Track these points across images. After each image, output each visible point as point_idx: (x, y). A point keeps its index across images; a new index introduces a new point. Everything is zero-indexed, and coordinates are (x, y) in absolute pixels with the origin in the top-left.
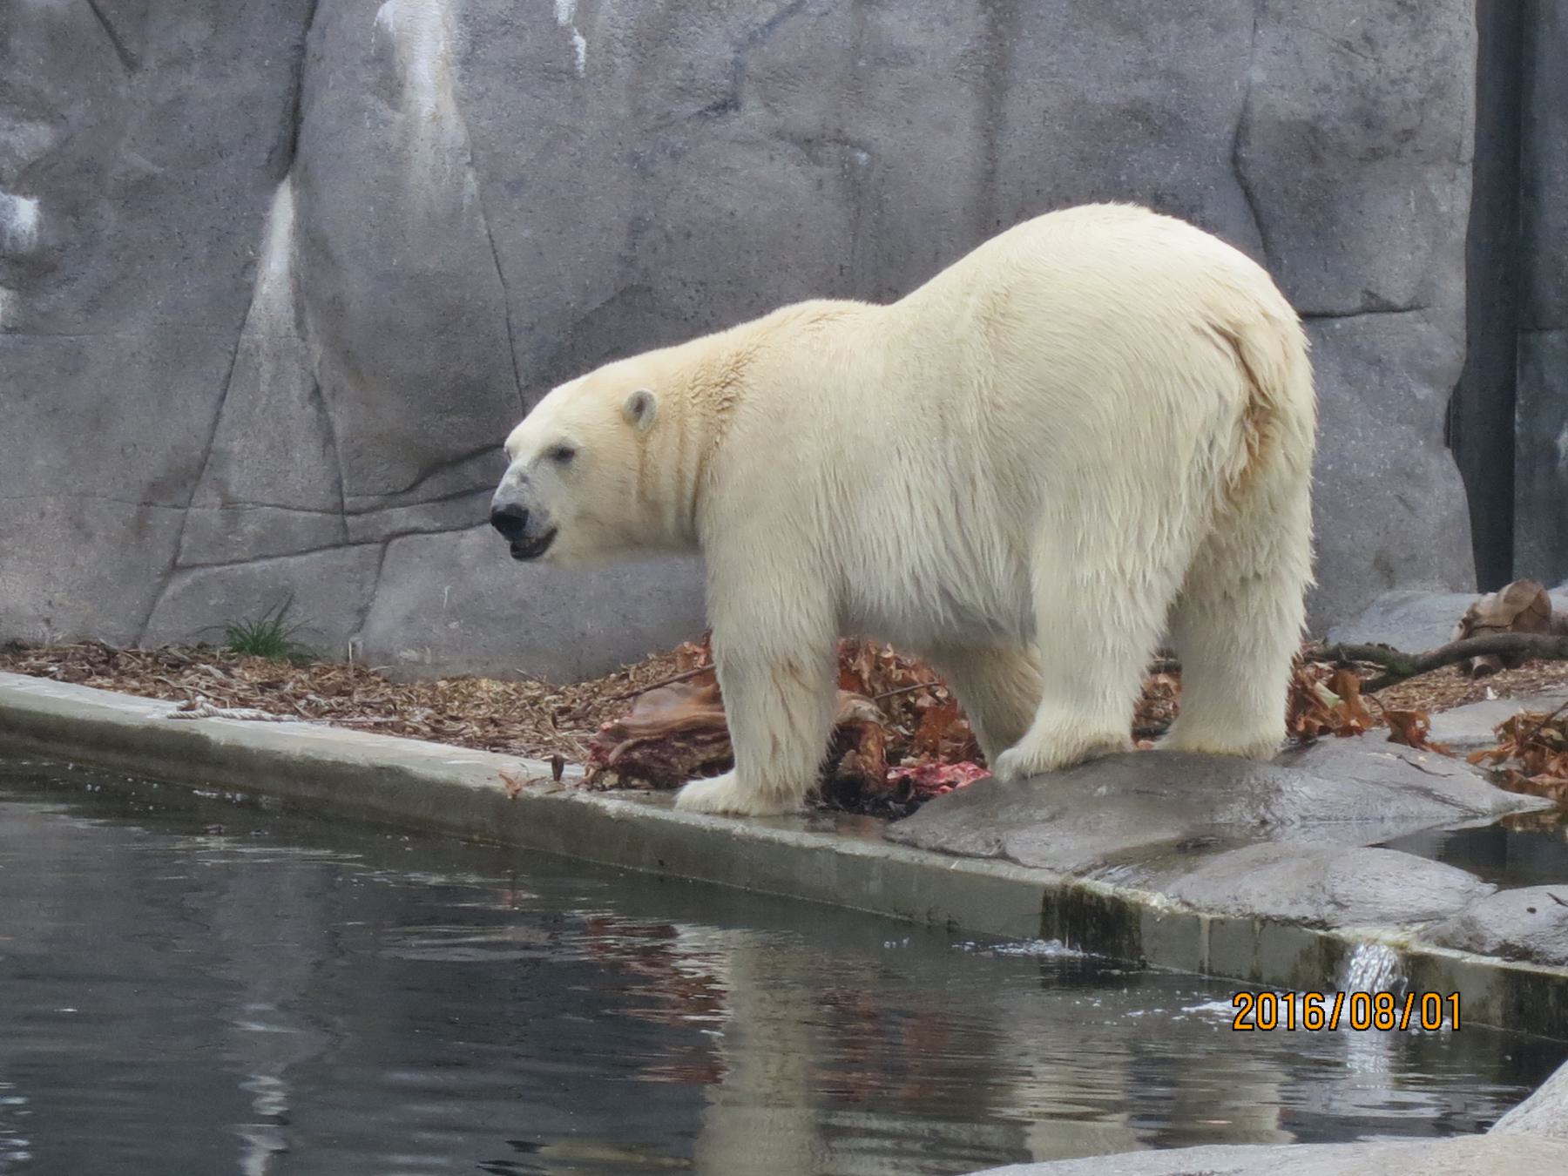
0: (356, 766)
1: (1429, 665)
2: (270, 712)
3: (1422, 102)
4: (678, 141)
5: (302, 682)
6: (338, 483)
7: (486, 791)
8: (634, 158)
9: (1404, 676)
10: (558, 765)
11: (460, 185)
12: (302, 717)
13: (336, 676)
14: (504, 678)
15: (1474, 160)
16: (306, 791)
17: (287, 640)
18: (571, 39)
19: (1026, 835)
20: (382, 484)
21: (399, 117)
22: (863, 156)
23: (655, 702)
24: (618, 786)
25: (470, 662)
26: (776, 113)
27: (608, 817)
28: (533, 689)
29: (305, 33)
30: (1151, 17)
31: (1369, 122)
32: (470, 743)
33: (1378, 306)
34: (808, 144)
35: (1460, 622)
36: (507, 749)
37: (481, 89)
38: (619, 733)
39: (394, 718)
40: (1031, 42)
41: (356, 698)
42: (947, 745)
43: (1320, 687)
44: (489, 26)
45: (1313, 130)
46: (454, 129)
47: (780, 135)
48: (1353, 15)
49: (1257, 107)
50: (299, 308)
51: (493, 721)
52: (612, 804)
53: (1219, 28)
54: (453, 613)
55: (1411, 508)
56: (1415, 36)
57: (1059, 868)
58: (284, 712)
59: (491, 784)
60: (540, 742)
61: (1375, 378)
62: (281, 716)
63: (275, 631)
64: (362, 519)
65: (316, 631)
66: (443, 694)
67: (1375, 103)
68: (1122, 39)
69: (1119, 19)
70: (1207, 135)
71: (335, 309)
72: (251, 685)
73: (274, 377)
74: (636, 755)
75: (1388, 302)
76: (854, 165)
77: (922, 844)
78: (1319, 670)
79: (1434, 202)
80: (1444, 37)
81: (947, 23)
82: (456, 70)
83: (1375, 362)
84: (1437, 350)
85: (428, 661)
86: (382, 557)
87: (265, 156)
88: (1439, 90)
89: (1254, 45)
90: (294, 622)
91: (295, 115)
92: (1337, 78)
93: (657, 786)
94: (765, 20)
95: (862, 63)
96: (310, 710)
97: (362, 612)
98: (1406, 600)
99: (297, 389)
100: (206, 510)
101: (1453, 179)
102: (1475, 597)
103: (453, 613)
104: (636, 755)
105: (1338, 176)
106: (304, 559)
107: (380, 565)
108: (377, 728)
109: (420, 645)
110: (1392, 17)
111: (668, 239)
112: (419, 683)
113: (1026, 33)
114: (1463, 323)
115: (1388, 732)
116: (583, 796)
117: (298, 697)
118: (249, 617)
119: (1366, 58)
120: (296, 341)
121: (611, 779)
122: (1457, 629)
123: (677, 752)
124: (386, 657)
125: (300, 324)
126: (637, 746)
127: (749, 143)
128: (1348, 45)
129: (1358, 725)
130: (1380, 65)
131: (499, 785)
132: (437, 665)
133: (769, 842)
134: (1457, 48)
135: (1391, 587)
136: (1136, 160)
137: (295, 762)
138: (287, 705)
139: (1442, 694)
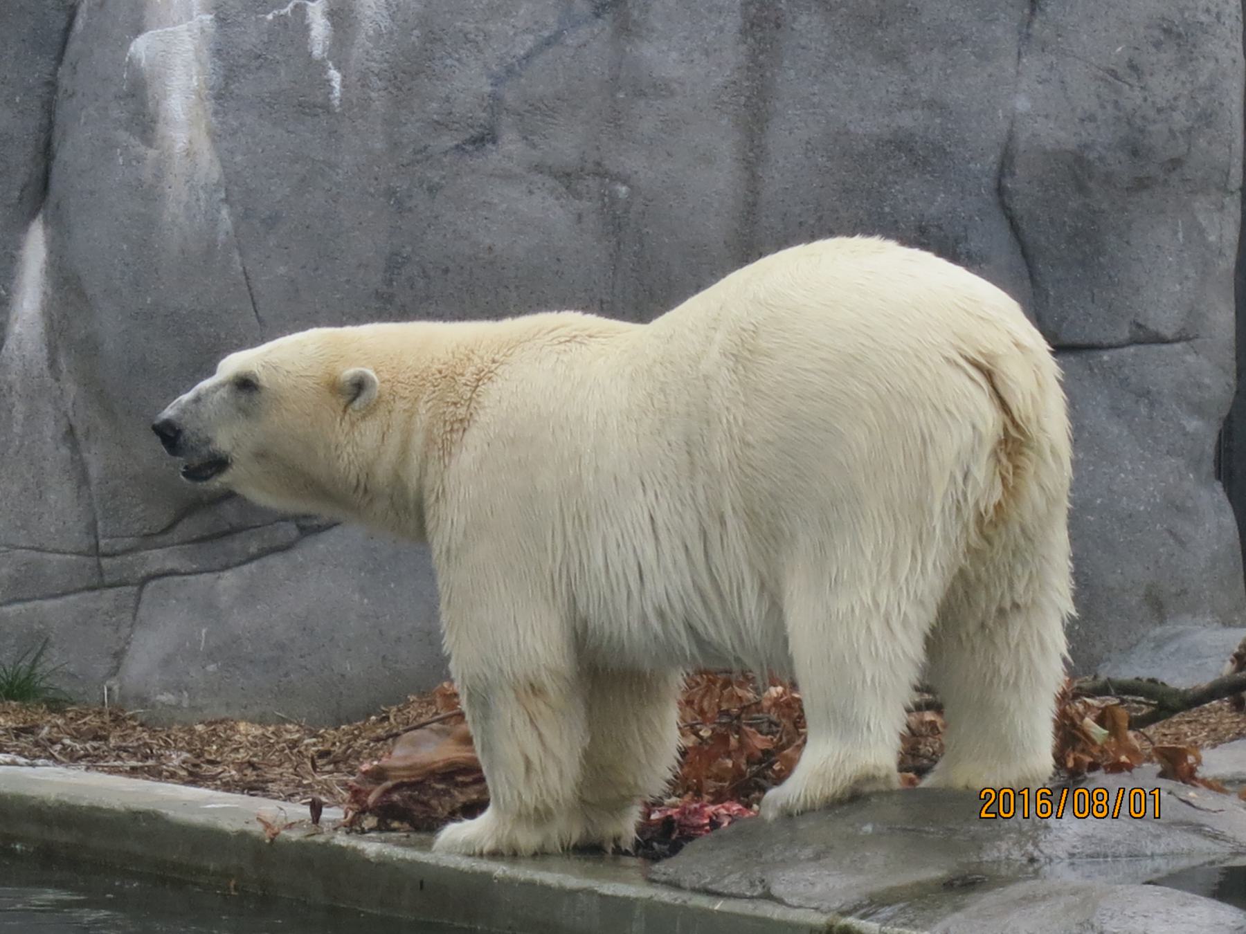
0: (112, 811)
1: (1195, 700)
2: (26, 757)
3: (1189, 130)
4: (434, 176)
5: (58, 726)
6: (92, 528)
7: (243, 835)
8: (391, 193)
9: (1174, 711)
10: (316, 808)
11: (214, 222)
12: (57, 762)
13: (93, 721)
14: (262, 721)
15: (1242, 189)
16: (61, 837)
17: (43, 684)
18: (326, 73)
19: (791, 874)
20: (137, 526)
21: (152, 153)
22: (623, 190)
23: (415, 743)
24: (378, 829)
25: (228, 705)
26: (534, 146)
27: (368, 861)
28: (292, 732)
29: (56, 69)
30: (913, 46)
32: (228, 787)
33: (1147, 337)
34: (567, 178)
35: (1232, 657)
36: (265, 793)
37: (235, 124)
38: (378, 775)
39: (150, 762)
40: (792, 72)
41: (113, 742)
42: (711, 785)
43: (1089, 722)
44: (243, 61)
46: (208, 166)
47: (538, 168)
48: (1118, 42)
49: (1023, 137)
50: (52, 348)
51: (252, 765)
52: (372, 847)
53: (983, 56)
54: (210, 656)
55: (1182, 543)
56: (1181, 64)
57: (825, 907)
58: (39, 757)
59: (249, 828)
60: (299, 785)
61: (1144, 411)
62: (35, 761)
63: (30, 676)
64: (118, 561)
65: (73, 676)
66: (200, 736)
67: (1142, 131)
68: (885, 68)
69: (882, 48)
70: (972, 165)
71: (89, 349)
72: (6, 730)
73: (26, 418)
74: (395, 797)
75: (1157, 334)
76: (614, 199)
77: (687, 885)
78: (1088, 707)
79: (1202, 232)
80: (1211, 65)
81: (707, 54)
82: (211, 105)
83: (1144, 394)
84: (1207, 381)
85: (185, 704)
86: (138, 600)
87: (17, 194)
88: (1207, 118)
89: (1018, 72)
90: (50, 666)
91: (47, 152)
92: (1103, 107)
93: (417, 829)
94: (522, 52)
95: (621, 96)
96: (65, 756)
97: (119, 655)
98: (1177, 635)
99: (50, 430)
101: (1222, 208)
103: (210, 656)
104: (395, 797)
105: (1105, 206)
106: (58, 602)
107: (136, 608)
108: (133, 772)
109: (178, 688)
110: (1158, 45)
111: (425, 275)
112: (176, 727)
113: (786, 63)
114: (1233, 355)
115: (1158, 768)
116: (341, 839)
117: (53, 742)
119: (1131, 86)
120: (49, 381)
121: (370, 821)
122: (1229, 663)
123: (438, 794)
124: (142, 701)
125: (53, 363)
126: (397, 788)
127: (508, 177)
128: (1113, 73)
129: (1128, 761)
130: (1146, 93)
131: (256, 829)
132: (193, 708)
133: (530, 884)
134: (1224, 75)
135: (1162, 620)
136: (900, 192)
137: (49, 808)
138: (42, 750)
139: (1215, 730)
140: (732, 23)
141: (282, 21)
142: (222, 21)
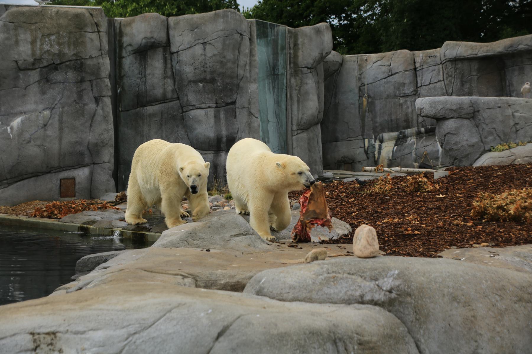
4: (23, 146)
8: (18, 148)
33: (104, 162)
34: (39, 146)
45: (96, 144)
47: (35, 145)
53: (86, 133)
102: (116, 194)
127: (32, 146)
140: (58, 129)
141: (4, 129)
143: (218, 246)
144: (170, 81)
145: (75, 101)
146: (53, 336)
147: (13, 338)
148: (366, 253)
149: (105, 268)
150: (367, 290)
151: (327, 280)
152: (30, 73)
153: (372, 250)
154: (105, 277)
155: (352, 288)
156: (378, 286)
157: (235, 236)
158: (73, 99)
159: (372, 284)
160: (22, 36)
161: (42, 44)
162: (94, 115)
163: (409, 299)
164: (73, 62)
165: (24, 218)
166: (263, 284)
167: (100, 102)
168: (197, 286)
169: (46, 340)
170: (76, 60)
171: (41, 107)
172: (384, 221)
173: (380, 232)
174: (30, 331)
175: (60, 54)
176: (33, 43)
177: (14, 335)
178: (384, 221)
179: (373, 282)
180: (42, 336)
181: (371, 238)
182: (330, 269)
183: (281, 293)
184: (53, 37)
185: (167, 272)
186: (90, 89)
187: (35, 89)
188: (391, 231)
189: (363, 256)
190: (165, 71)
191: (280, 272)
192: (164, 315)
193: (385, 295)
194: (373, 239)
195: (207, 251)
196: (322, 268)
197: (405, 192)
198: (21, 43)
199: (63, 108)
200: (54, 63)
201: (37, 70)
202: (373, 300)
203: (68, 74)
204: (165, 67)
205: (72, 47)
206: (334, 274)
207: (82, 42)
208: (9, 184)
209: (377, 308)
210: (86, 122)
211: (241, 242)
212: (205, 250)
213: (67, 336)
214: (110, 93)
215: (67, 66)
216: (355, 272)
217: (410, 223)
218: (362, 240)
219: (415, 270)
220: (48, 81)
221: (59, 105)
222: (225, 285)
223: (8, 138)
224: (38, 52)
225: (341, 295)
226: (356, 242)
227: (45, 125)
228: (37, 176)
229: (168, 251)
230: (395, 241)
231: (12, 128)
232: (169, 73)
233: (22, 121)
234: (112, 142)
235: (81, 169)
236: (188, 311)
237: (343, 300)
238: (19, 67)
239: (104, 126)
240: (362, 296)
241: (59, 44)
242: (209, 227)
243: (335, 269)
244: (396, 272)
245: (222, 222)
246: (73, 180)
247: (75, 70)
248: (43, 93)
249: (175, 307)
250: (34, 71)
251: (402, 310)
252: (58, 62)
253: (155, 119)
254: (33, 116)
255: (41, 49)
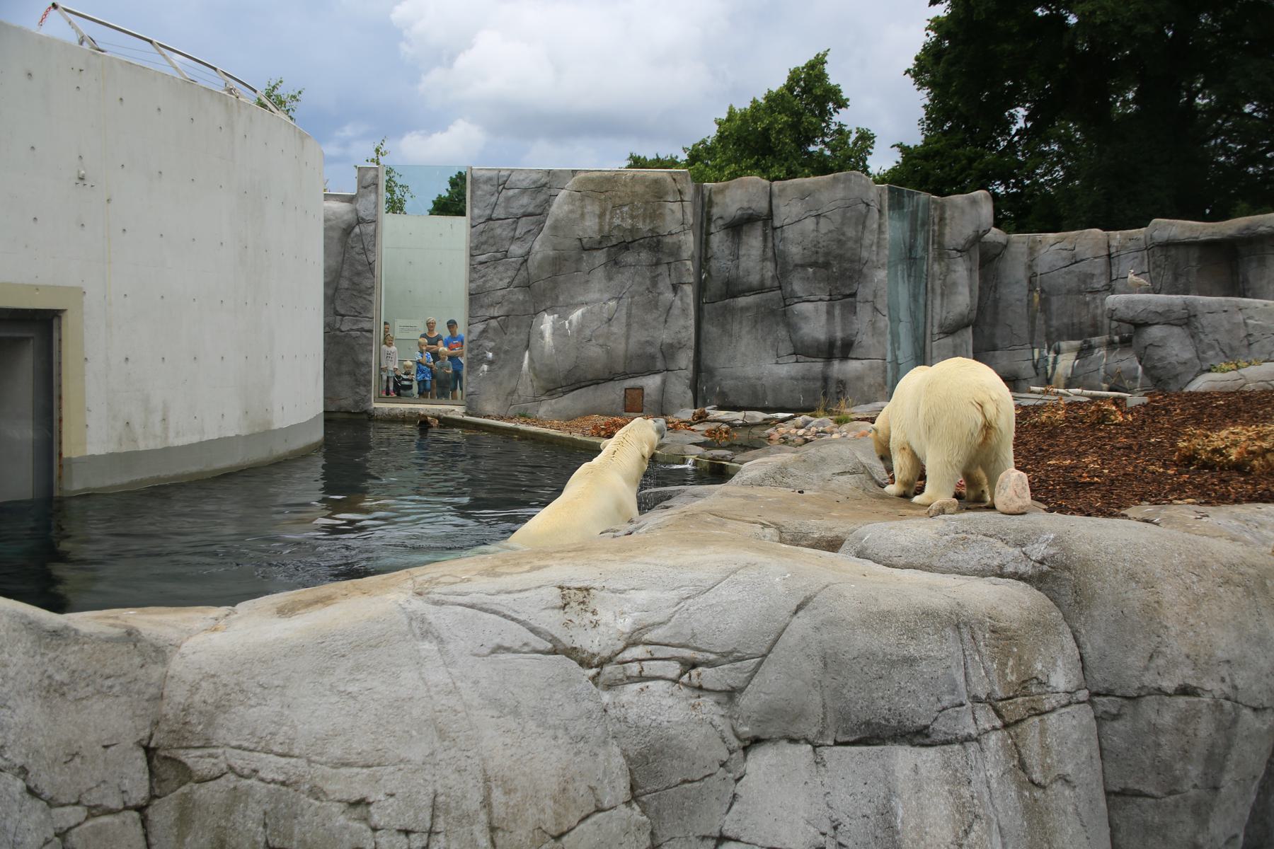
31: (679, 343)
33: (680, 369)
46: (552, 344)
53: (659, 330)
71: (534, 369)
83: (680, 377)
91: (529, 341)
99: (529, 380)
100: (516, 397)
118: (521, 412)
142: (553, 323)
143: (815, 487)
144: (770, 266)
145: (648, 289)
146: (585, 593)
147: (538, 590)
148: (1013, 507)
149: (667, 508)
150: (1009, 559)
151: (955, 542)
152: (596, 253)
153: (1021, 504)
154: (662, 520)
155: (988, 555)
156: (1025, 554)
157: (838, 474)
158: (645, 287)
159: (1017, 551)
160: (589, 208)
161: (612, 218)
162: (670, 308)
163: (1067, 574)
164: (648, 239)
165: (578, 436)
166: (866, 542)
167: (679, 292)
168: (782, 541)
169: (577, 597)
170: (652, 237)
171: (607, 296)
172: (1051, 462)
173: (1043, 478)
174: (560, 584)
175: (633, 230)
176: (602, 215)
177: (539, 587)
178: (1051, 462)
179: (1019, 549)
180: (572, 592)
181: (1020, 487)
182: (959, 527)
183: (890, 557)
184: (625, 209)
185: (743, 518)
186: (667, 273)
187: (600, 273)
188: (1059, 477)
189: (1007, 511)
190: (764, 251)
191: (890, 529)
192: (728, 577)
193: (1033, 566)
194: (1023, 488)
195: (799, 492)
196: (948, 526)
197: (1084, 423)
198: (587, 217)
199: (632, 297)
200: (624, 242)
201: (604, 250)
202: (1016, 573)
203: (641, 254)
204: (765, 246)
205: (648, 221)
206: (964, 535)
207: (660, 214)
208: (565, 393)
209: (1022, 584)
210: (660, 316)
211: (846, 482)
212: (797, 491)
213: (602, 594)
214: (692, 280)
215: (640, 244)
216: (994, 533)
217: (1087, 467)
218: (1008, 490)
219: (1079, 534)
220: (616, 263)
221: (627, 294)
222: (819, 540)
223: (566, 335)
224: (607, 228)
225: (972, 563)
226: (999, 492)
227: (610, 320)
228: (598, 384)
229: (749, 491)
230: (1063, 490)
231: (570, 323)
232: (770, 254)
233: (583, 314)
234: (692, 343)
235: (651, 376)
236: (759, 573)
237: (975, 570)
238: (583, 247)
239: (682, 322)
240: (1001, 567)
241: (632, 217)
242: (804, 461)
243: (966, 528)
244: (1052, 536)
245: (822, 455)
246: (641, 391)
247: (650, 250)
248: (610, 279)
249: (742, 568)
250: (601, 251)
251: (1056, 588)
252: (630, 240)
253: (748, 314)
254: (596, 308)
255: (610, 224)
